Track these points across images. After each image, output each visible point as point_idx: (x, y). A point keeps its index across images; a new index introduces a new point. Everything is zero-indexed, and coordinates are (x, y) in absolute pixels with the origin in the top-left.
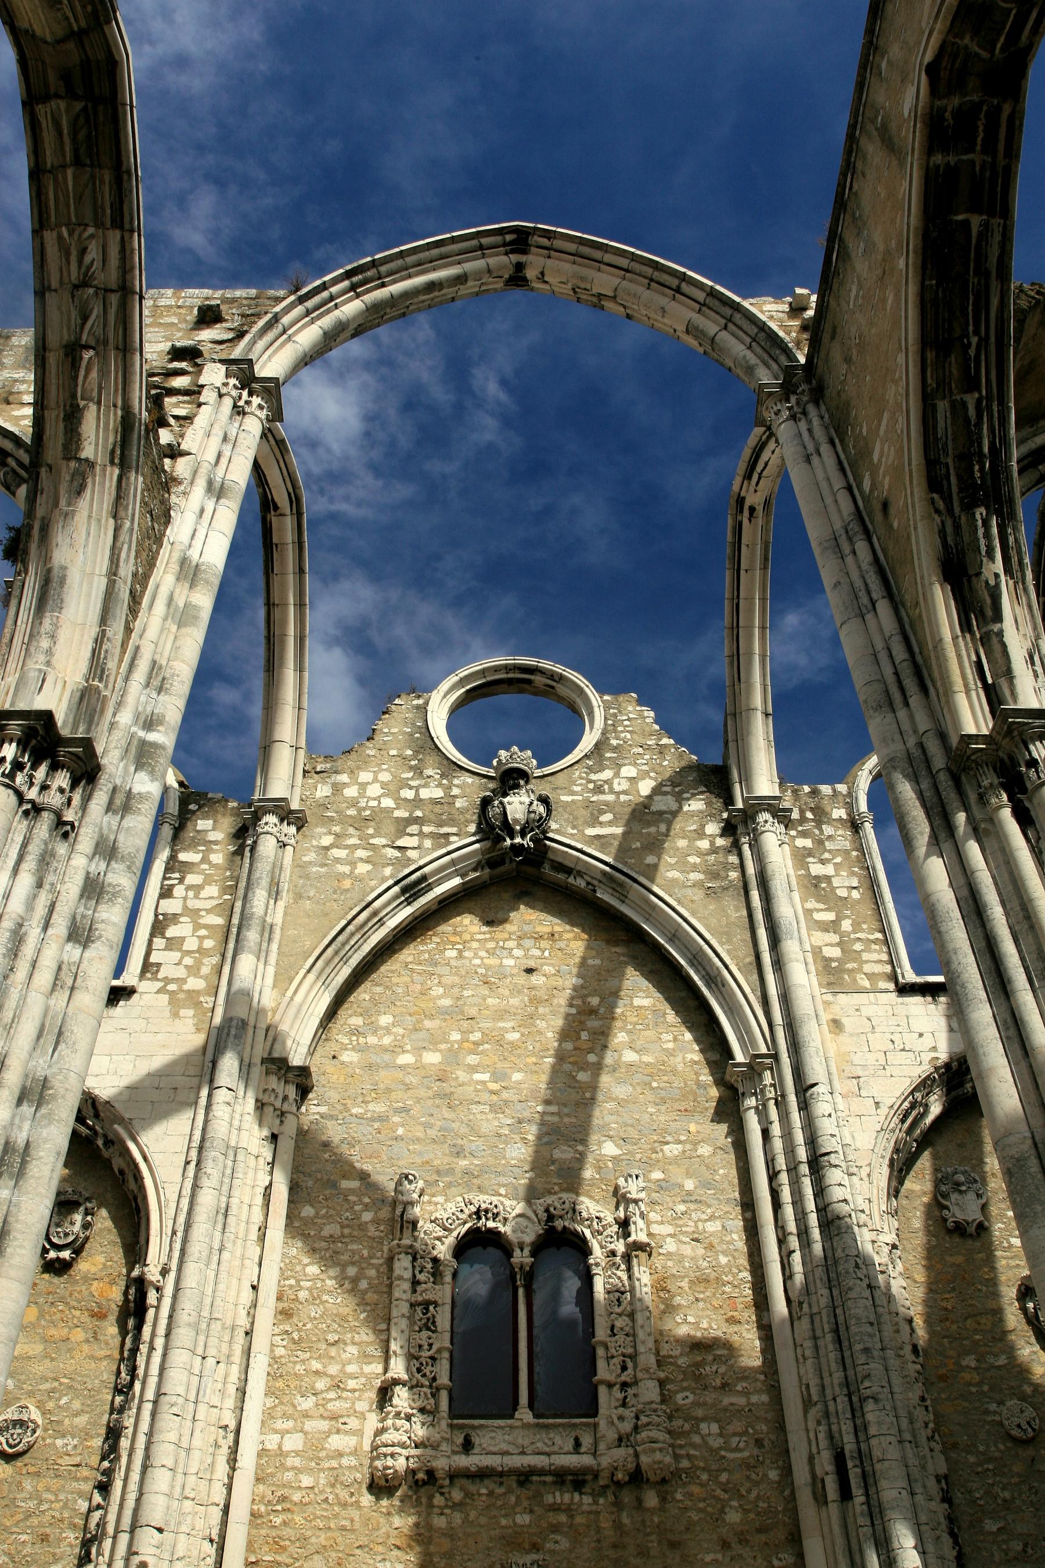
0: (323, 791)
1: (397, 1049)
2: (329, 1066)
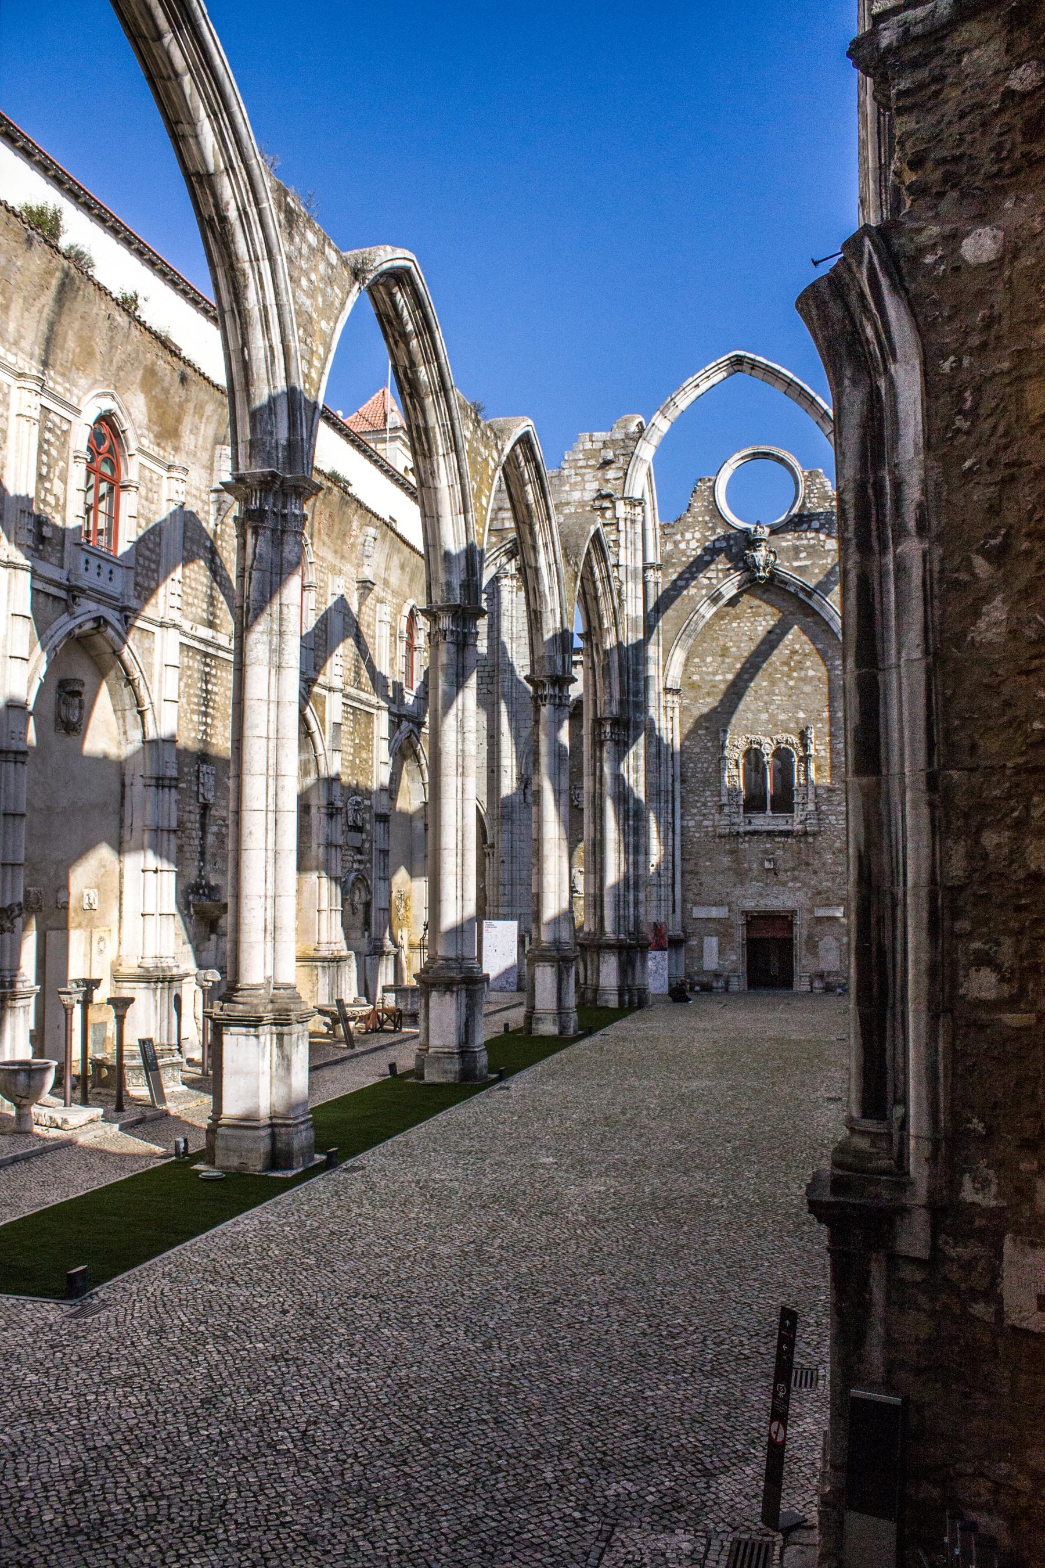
0: (669, 547)
1: (715, 674)
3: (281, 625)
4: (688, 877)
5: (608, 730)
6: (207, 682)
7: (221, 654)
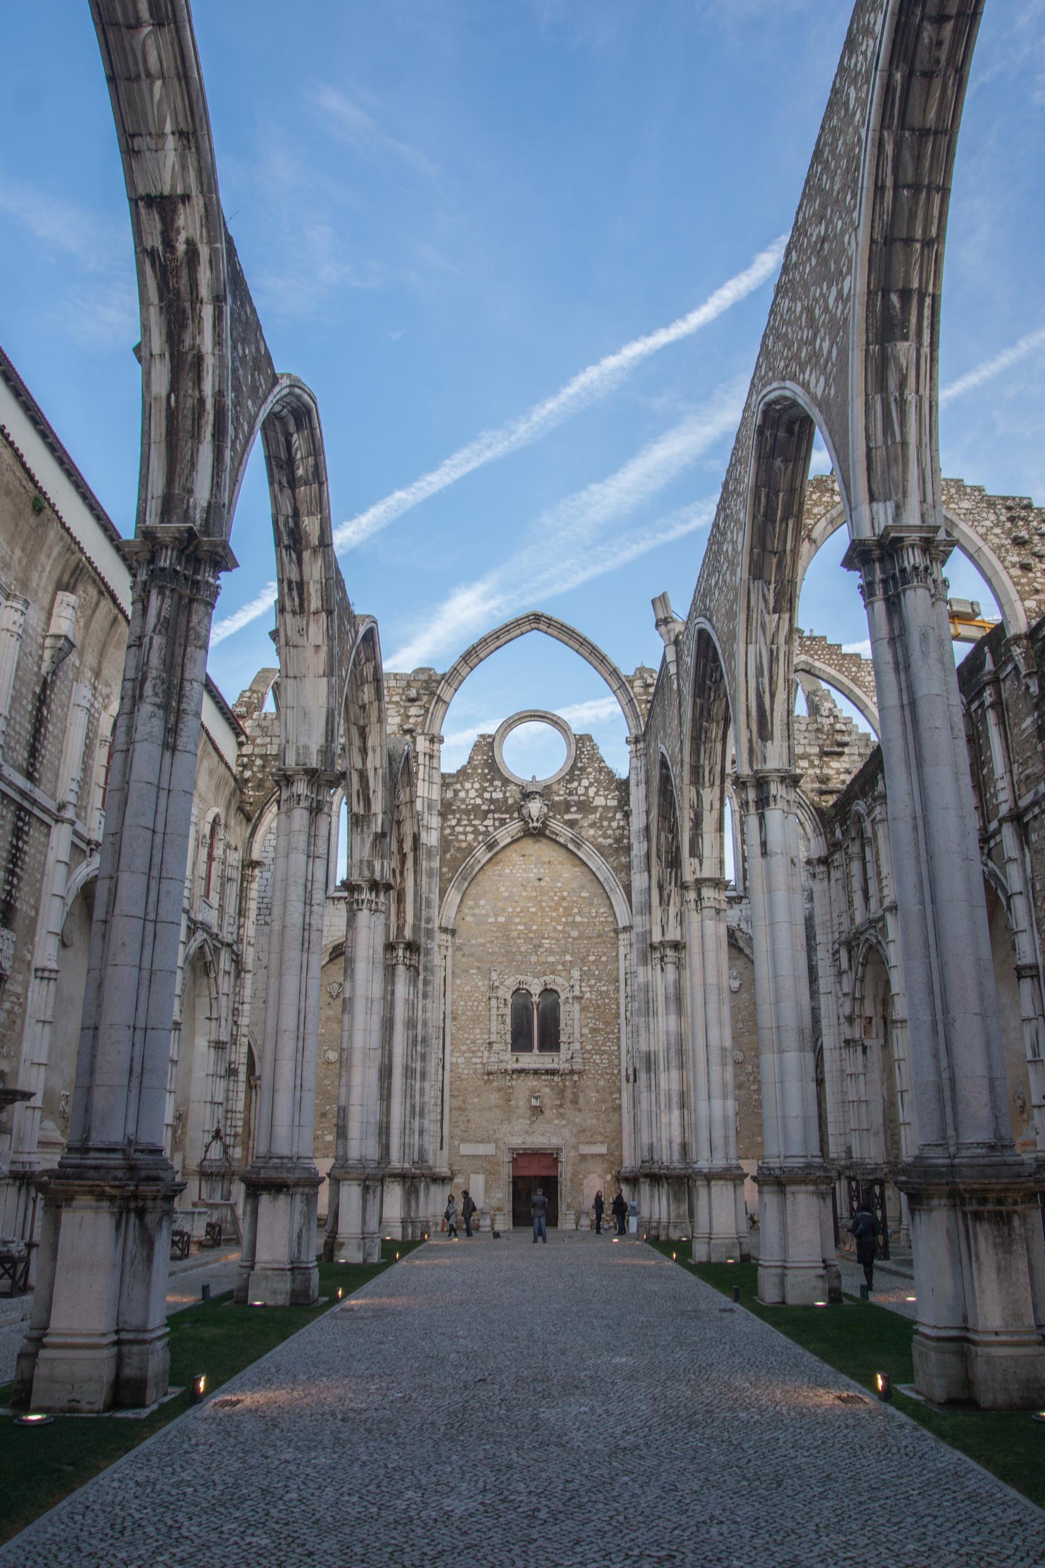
1: (487, 915)
2: (462, 923)
3: (179, 702)
4: (456, 1113)
5: (401, 953)
6: (18, 838)
7: (36, 811)
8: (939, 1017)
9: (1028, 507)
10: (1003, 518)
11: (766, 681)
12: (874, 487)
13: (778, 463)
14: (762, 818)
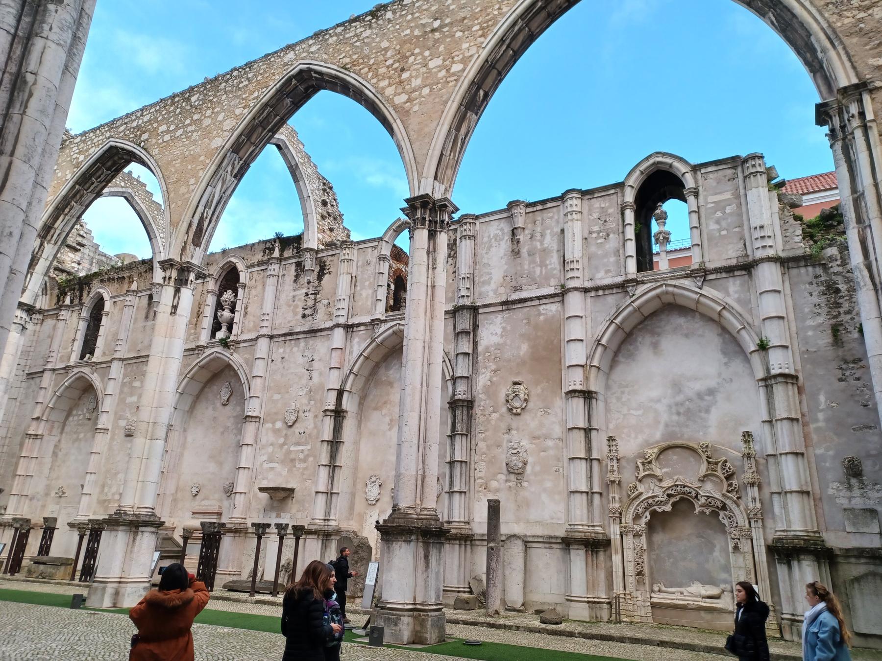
8: (421, 442)
9: (331, 188)
10: (320, 187)
11: (210, 212)
12: (439, 174)
13: (288, 101)
14: (177, 291)
